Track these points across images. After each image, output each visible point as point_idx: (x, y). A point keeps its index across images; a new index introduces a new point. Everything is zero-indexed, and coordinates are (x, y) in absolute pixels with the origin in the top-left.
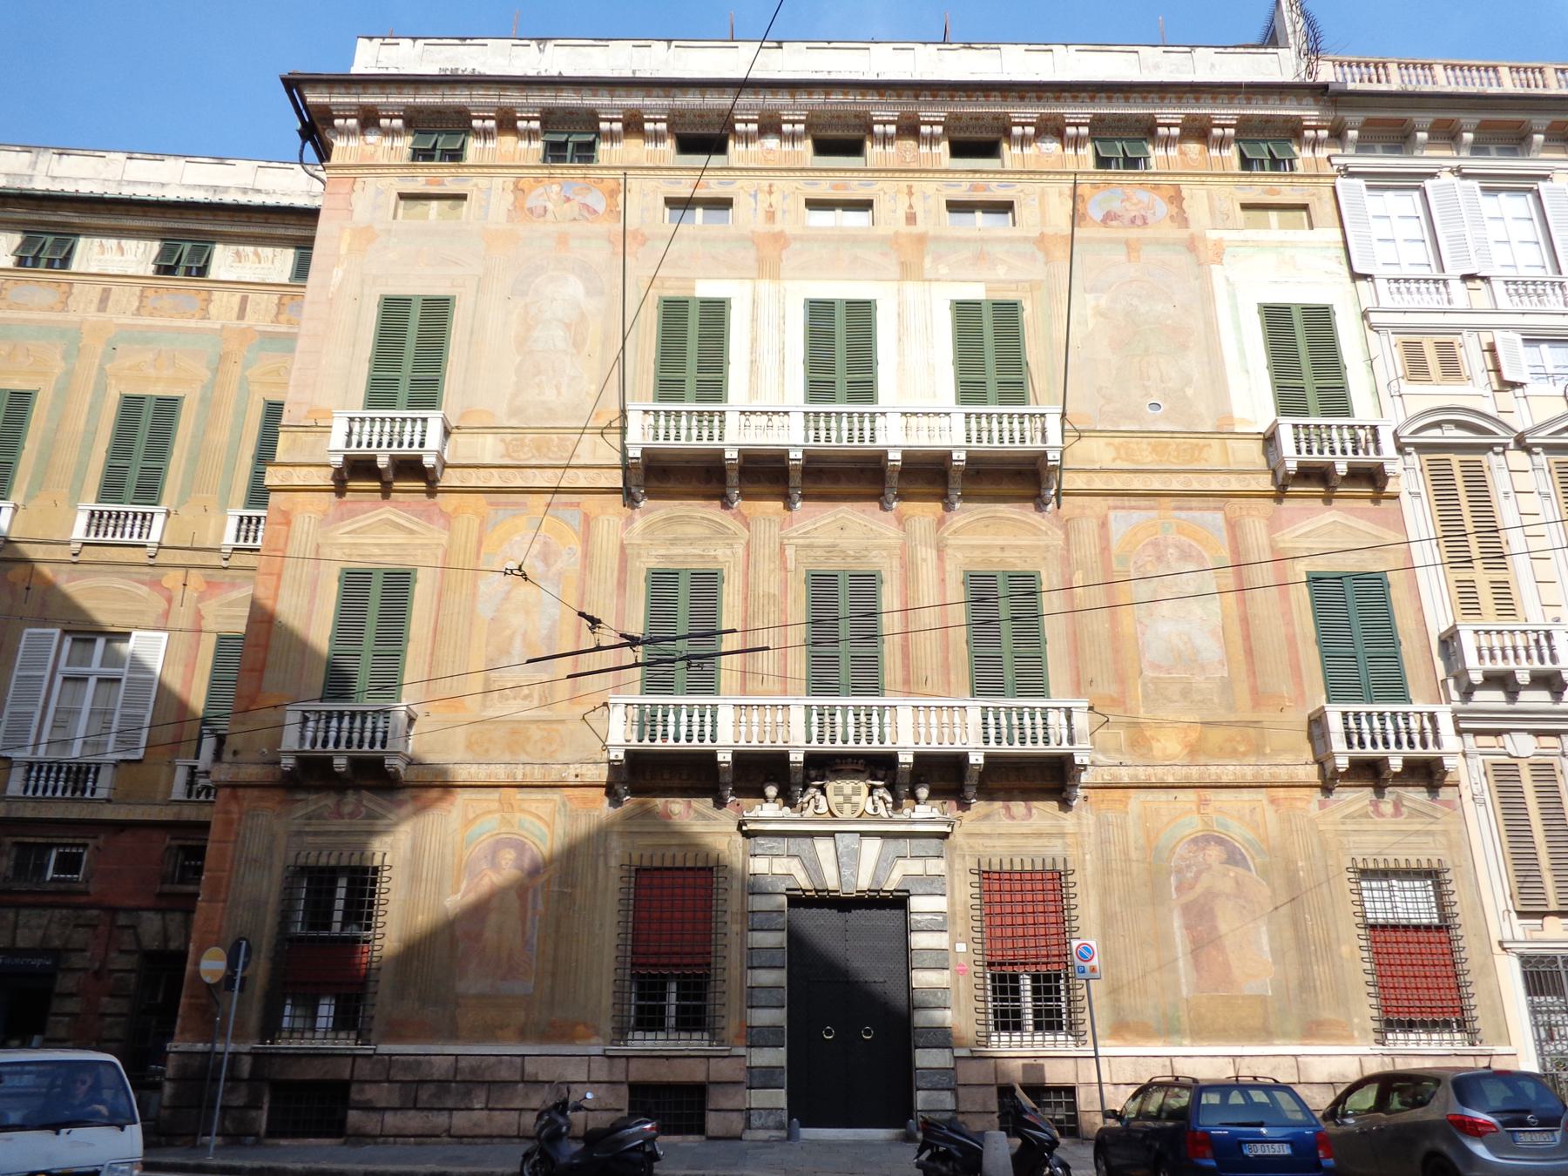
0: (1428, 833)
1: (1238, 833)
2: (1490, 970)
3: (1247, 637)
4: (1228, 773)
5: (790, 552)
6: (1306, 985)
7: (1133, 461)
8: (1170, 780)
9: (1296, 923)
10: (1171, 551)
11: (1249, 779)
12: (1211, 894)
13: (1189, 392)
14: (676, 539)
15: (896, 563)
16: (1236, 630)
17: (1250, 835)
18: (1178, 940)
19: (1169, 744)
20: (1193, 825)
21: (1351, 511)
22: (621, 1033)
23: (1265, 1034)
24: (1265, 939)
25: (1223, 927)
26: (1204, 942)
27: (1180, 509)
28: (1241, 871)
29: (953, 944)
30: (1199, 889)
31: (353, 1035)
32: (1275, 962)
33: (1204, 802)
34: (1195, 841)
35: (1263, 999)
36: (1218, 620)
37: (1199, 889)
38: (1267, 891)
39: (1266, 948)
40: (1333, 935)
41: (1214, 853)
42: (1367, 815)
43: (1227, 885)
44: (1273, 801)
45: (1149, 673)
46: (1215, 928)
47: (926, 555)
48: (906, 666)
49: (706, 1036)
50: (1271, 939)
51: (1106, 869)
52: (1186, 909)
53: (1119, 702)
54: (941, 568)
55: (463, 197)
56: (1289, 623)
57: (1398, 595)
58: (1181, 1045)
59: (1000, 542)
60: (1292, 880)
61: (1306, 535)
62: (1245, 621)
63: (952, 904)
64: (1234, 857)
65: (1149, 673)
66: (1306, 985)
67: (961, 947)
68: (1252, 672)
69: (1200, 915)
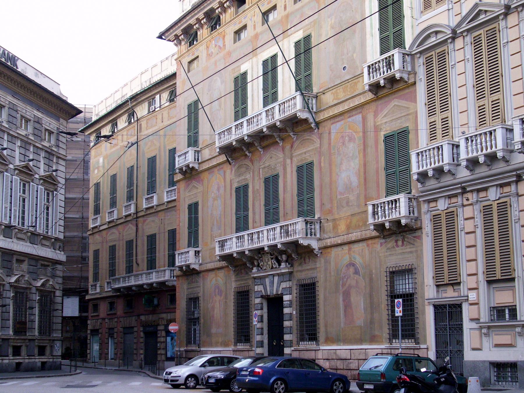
0: (411, 252)
1: (358, 260)
2: (424, 313)
3: (365, 173)
4: (354, 236)
5: (261, 170)
6: (372, 322)
7: (338, 99)
8: (339, 242)
9: (371, 296)
10: (347, 138)
11: (359, 238)
12: (350, 287)
13: (355, 55)
14: (240, 174)
15: (282, 168)
16: (362, 170)
17: (361, 261)
18: (341, 305)
19: (342, 227)
20: (346, 260)
21: (400, 98)
22: (235, 345)
23: (361, 341)
24: (362, 304)
25: (352, 299)
26: (348, 306)
27: (350, 117)
28: (357, 276)
29: (293, 310)
30: (347, 285)
31: (413, 340)
32: (365, 313)
33: (350, 249)
34: (347, 266)
35: (361, 327)
36: (357, 167)
37: (347, 285)
38: (364, 284)
39: (363, 308)
40: (380, 301)
41: (352, 270)
42: (394, 247)
43: (353, 283)
44: (368, 246)
45: (339, 197)
46: (350, 300)
47: (288, 161)
48: (284, 209)
49: (413, 340)
50: (364, 303)
51: (326, 280)
52: (344, 293)
53: (330, 212)
54: (292, 167)
55: (198, 57)
56: (377, 162)
57: (411, 136)
58: (340, 345)
59: (305, 151)
60: (371, 279)
61: (385, 116)
62: (365, 165)
63: (293, 297)
64: (356, 272)
65: (339, 197)
66: (372, 322)
67: (294, 313)
68: (366, 189)
69: (347, 295)
